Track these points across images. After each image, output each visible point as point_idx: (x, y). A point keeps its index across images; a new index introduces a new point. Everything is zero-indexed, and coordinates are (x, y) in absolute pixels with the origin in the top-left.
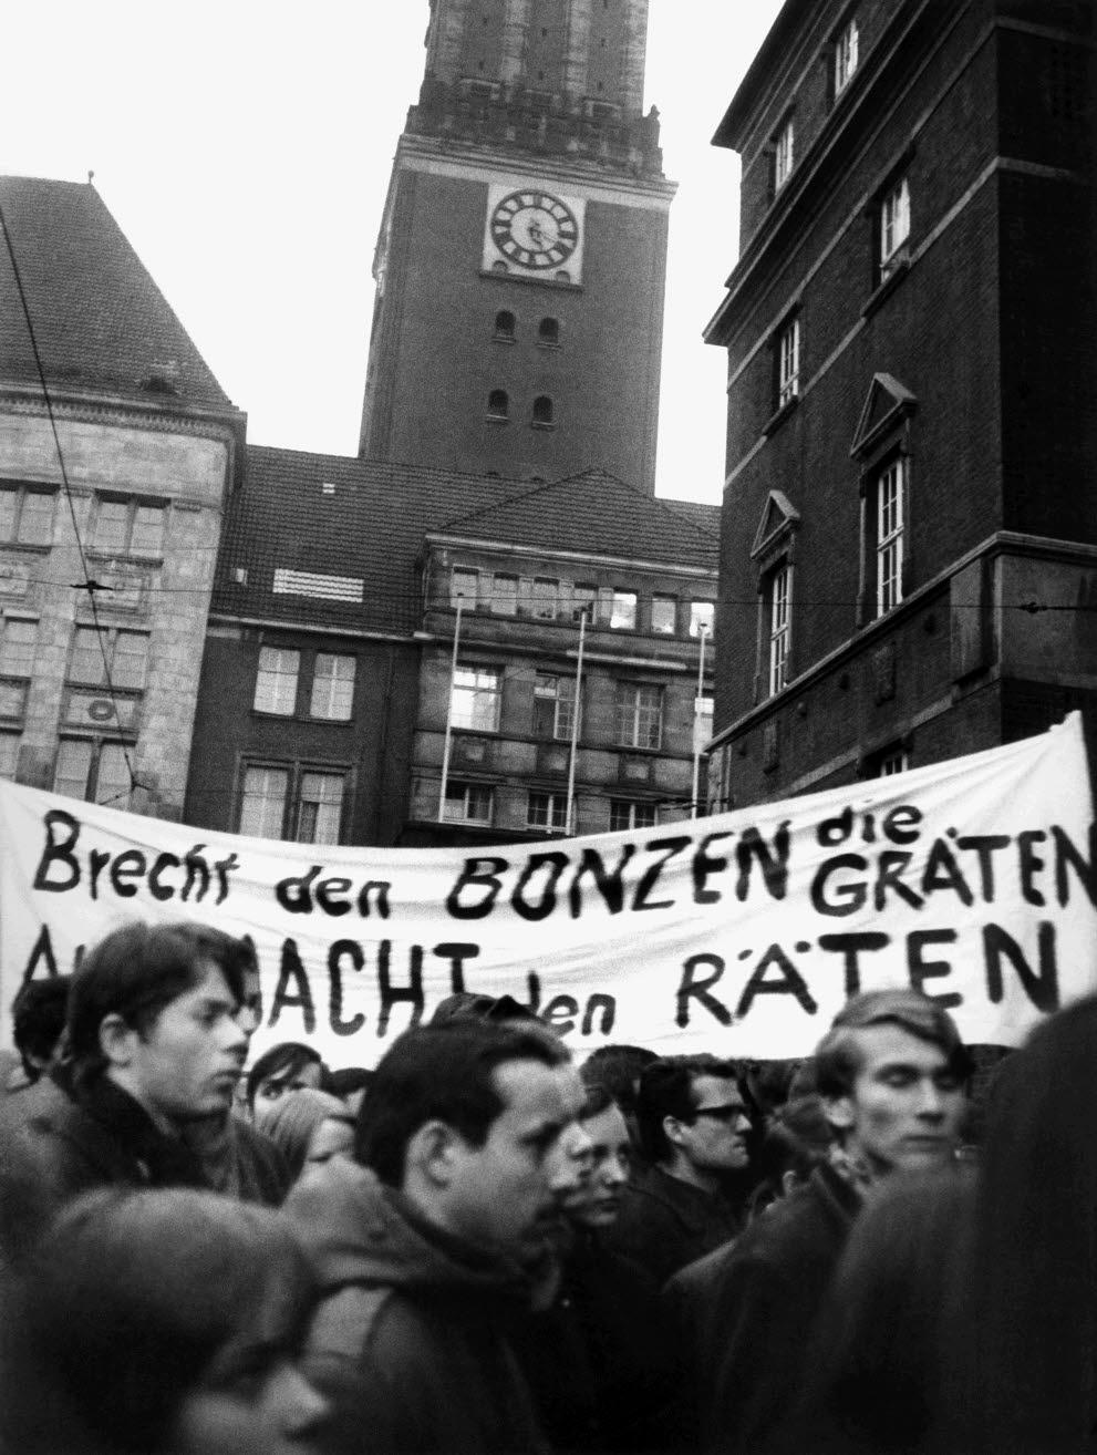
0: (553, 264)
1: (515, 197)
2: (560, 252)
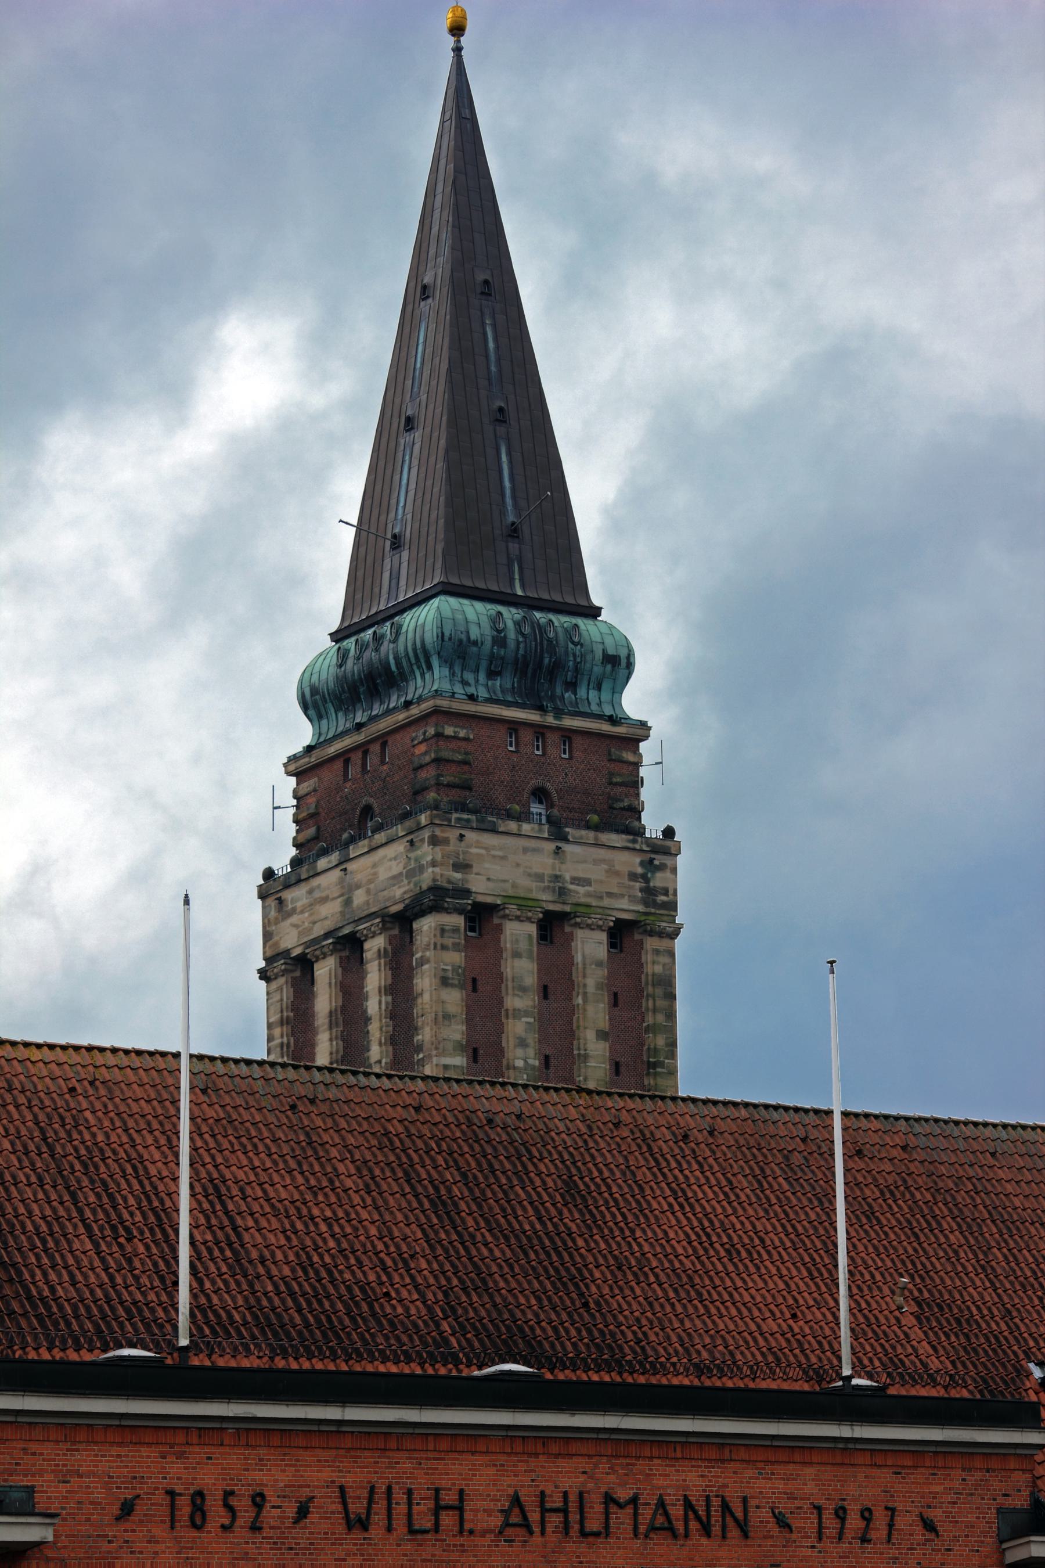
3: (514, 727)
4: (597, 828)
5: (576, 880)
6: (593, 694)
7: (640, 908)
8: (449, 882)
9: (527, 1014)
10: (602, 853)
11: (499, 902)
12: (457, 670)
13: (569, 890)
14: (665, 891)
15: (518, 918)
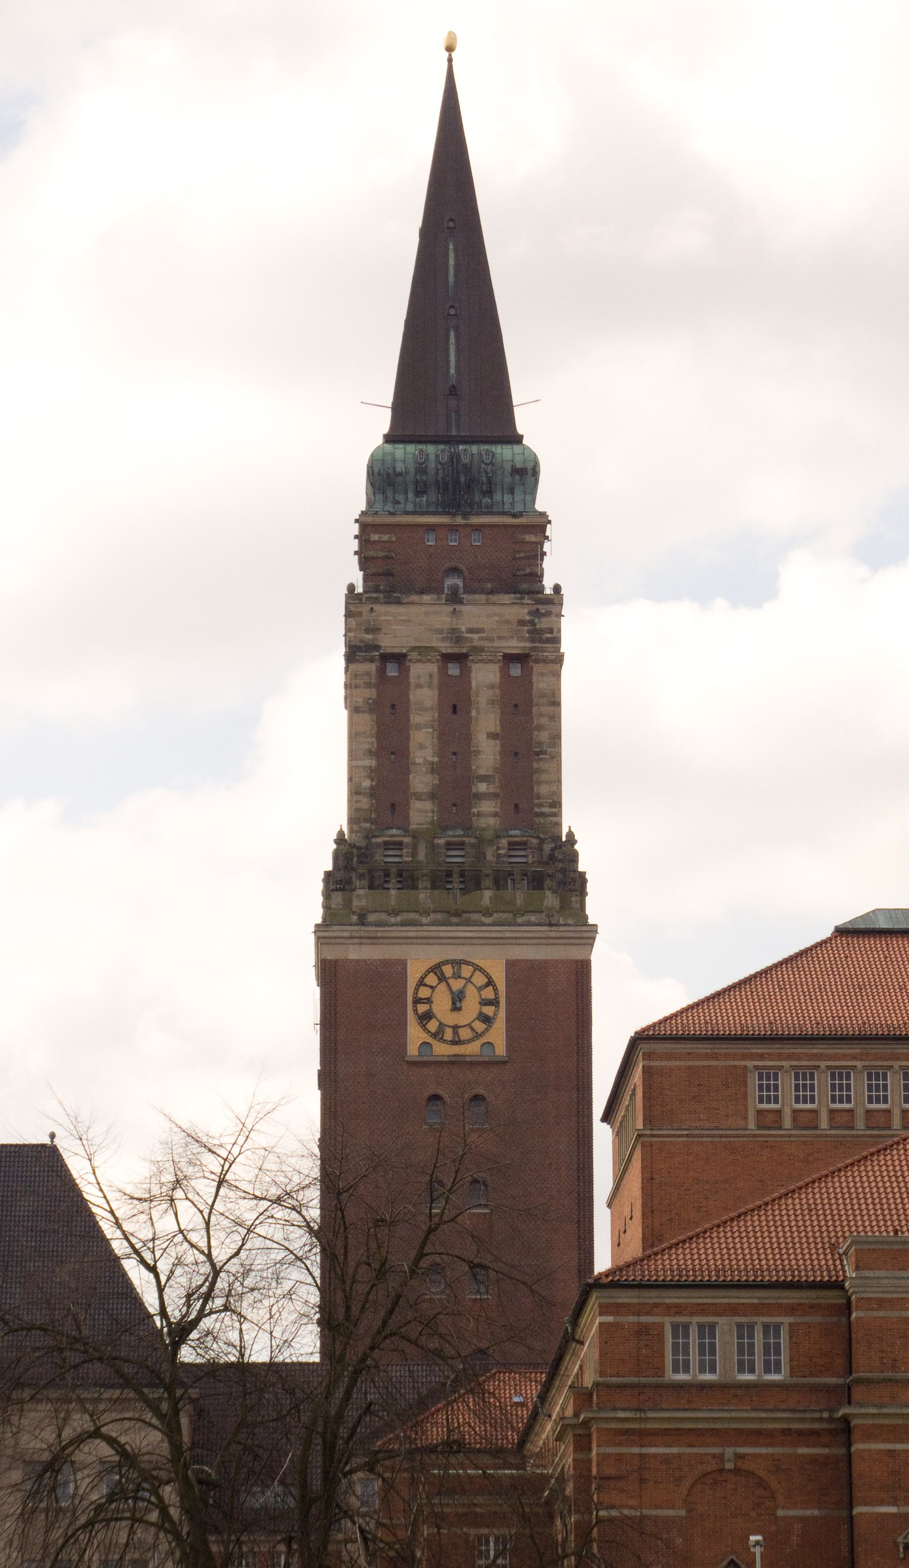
0: (478, 1036)
1: (436, 969)
2: (484, 1022)
3: (431, 528)
4: (492, 592)
5: (471, 631)
6: (507, 498)
7: (528, 645)
8: (362, 641)
9: (426, 726)
10: (497, 609)
11: (405, 651)
12: (389, 494)
13: (465, 639)
14: (551, 631)
15: (420, 661)
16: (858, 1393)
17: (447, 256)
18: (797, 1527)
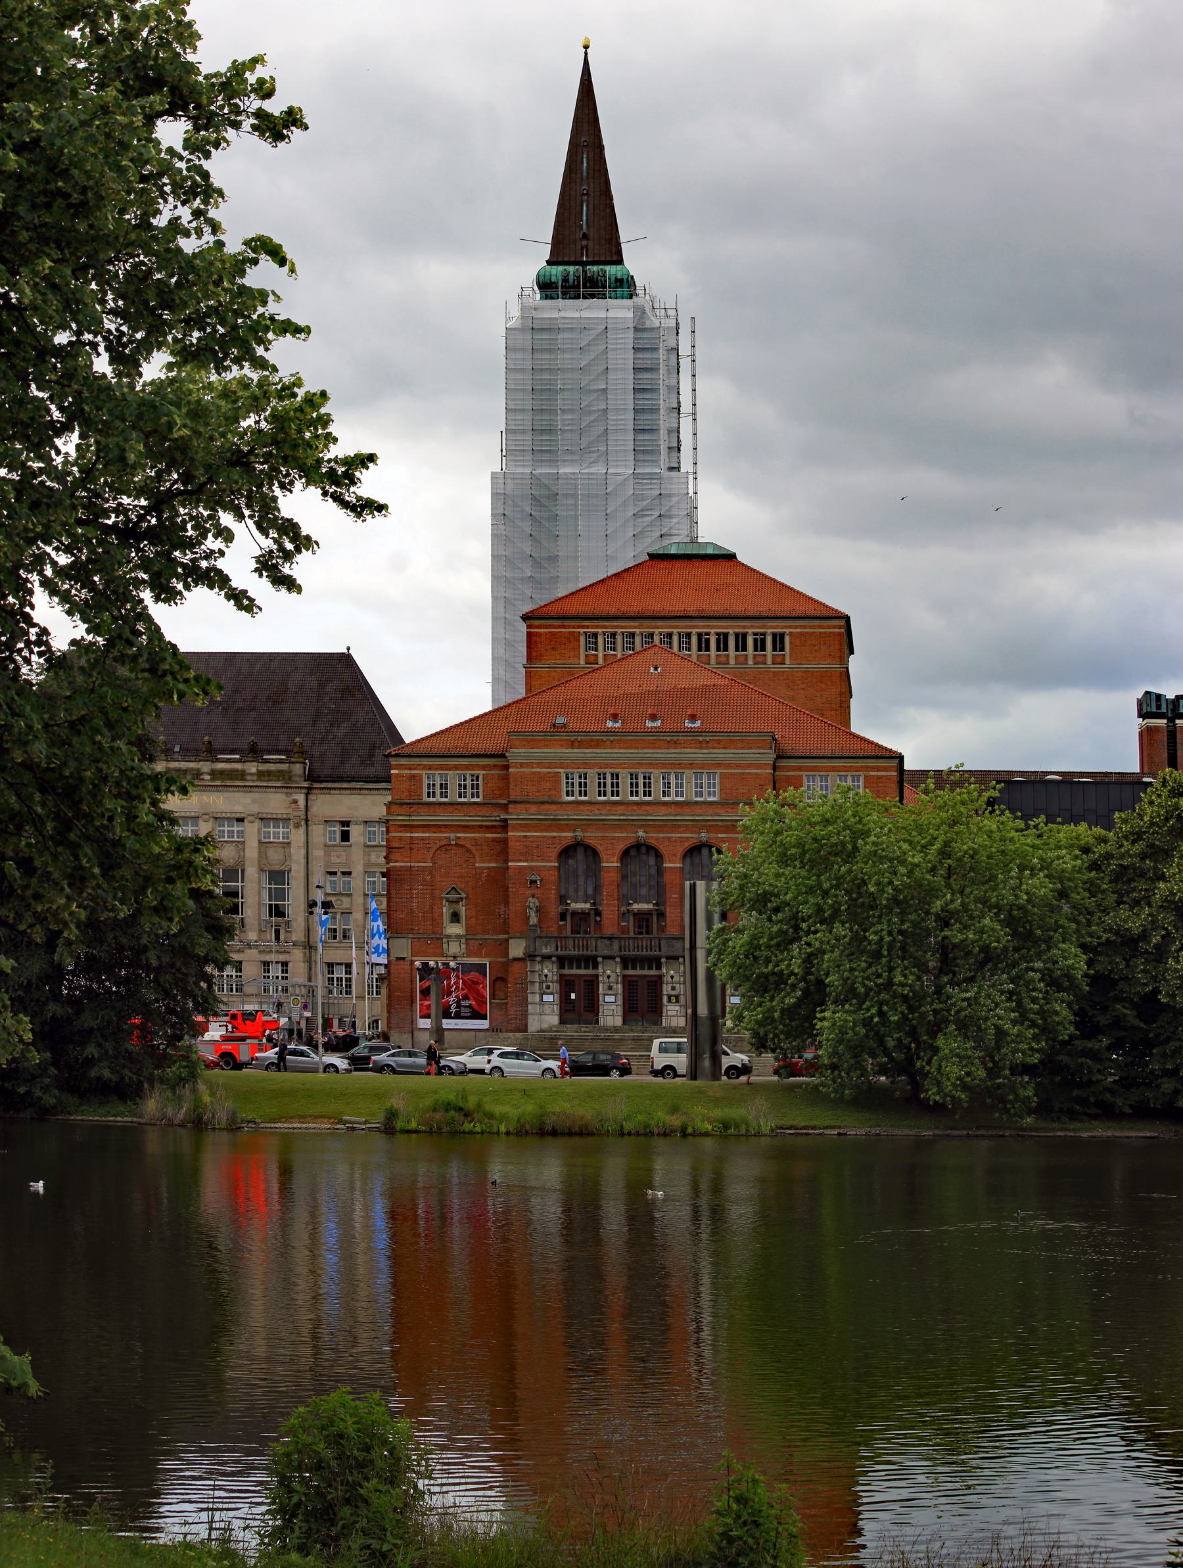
16: (511, 807)
17: (582, 163)
18: (485, 871)
